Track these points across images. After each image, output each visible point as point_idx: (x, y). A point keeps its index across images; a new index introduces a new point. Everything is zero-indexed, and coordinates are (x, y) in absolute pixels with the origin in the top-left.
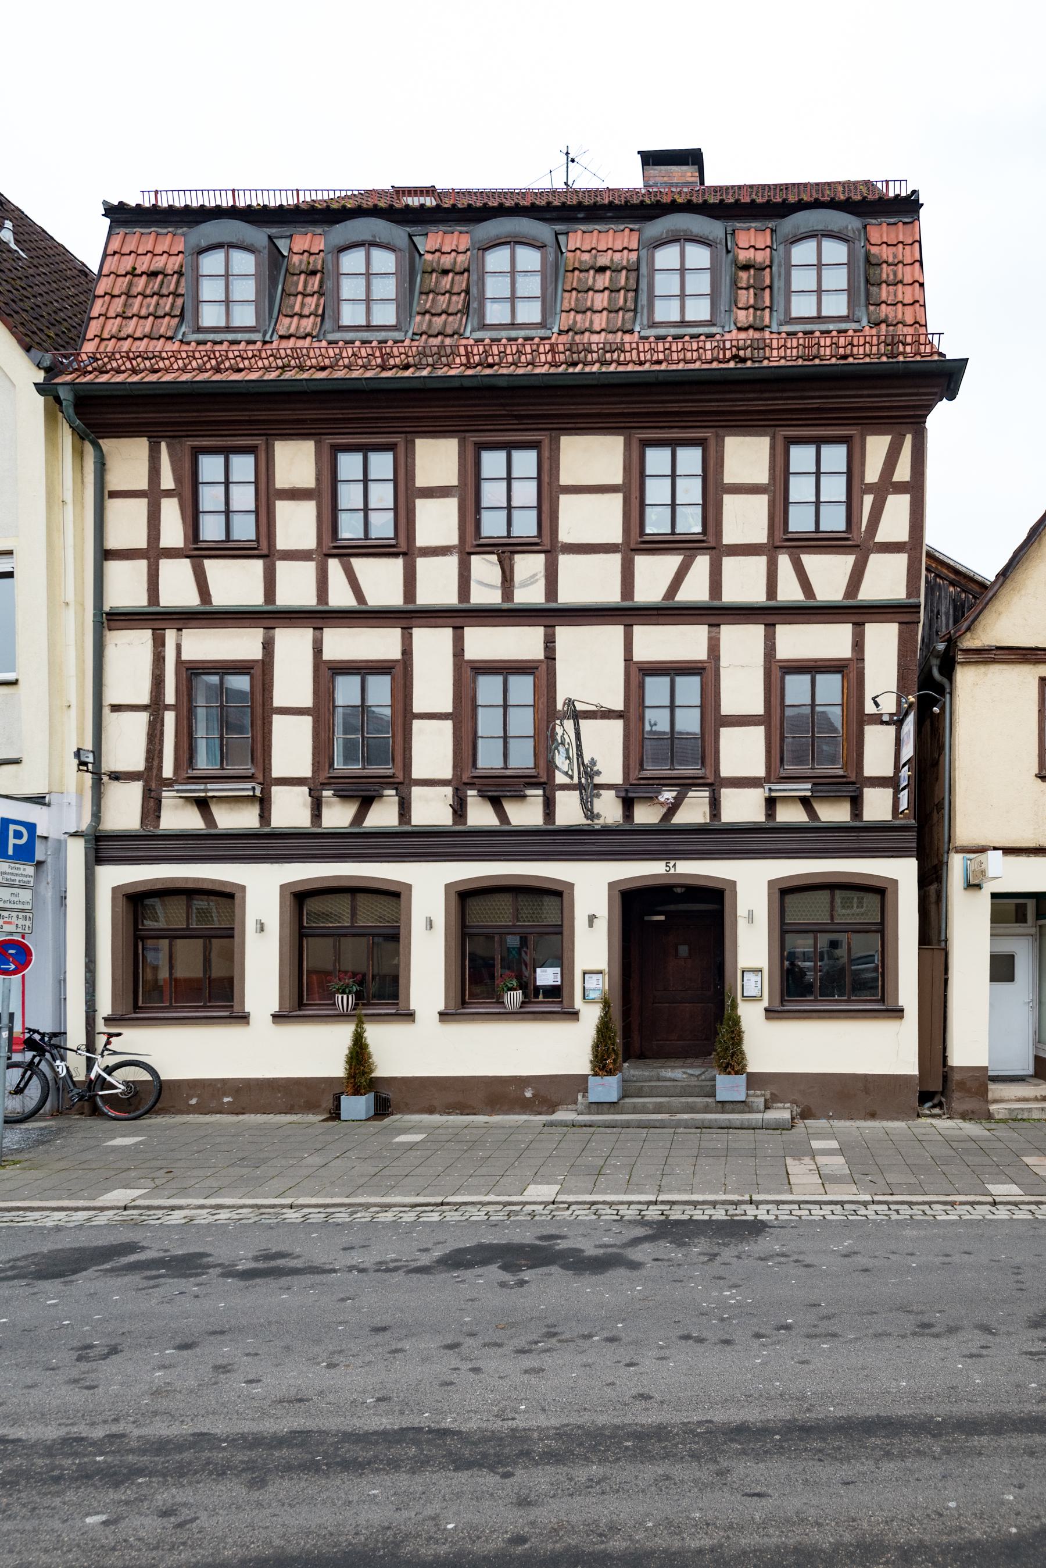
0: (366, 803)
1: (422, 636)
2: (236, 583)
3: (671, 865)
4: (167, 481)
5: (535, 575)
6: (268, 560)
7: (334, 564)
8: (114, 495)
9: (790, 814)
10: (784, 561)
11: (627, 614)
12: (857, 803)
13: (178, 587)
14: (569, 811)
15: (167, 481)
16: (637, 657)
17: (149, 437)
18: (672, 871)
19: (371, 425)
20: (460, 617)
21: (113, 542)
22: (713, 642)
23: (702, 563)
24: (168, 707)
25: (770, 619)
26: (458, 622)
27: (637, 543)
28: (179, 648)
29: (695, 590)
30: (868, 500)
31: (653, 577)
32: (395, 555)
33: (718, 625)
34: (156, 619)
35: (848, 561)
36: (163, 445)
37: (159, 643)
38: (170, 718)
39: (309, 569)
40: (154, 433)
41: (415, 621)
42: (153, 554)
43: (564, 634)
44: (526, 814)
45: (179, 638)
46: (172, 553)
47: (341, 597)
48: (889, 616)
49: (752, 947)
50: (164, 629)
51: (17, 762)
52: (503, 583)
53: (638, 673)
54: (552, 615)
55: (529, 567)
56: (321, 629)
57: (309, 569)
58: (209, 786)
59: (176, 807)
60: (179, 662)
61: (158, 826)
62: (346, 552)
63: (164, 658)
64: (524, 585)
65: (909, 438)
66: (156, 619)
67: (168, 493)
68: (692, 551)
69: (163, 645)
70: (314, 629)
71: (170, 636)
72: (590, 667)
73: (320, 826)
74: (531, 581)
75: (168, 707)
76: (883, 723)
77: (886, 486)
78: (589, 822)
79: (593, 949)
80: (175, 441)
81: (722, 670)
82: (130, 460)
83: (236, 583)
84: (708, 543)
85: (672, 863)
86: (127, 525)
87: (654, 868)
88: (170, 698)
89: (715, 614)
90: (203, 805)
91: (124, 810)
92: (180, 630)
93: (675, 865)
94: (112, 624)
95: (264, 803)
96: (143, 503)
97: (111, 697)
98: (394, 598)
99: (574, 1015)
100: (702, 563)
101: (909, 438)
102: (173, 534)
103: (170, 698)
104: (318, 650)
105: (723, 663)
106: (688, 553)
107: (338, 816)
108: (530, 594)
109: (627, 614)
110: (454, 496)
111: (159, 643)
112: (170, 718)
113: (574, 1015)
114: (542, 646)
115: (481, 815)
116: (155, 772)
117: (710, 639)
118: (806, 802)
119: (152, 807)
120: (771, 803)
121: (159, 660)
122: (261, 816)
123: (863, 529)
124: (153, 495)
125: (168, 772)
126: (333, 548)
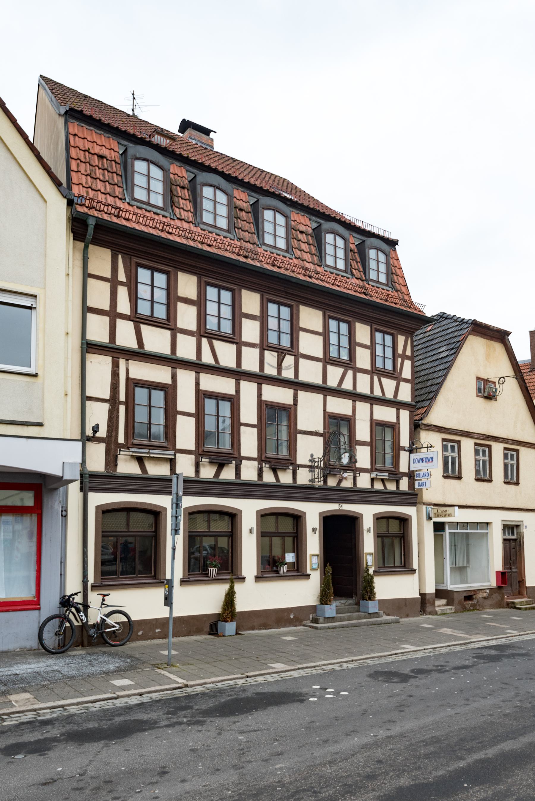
0: (221, 467)
2: (156, 340)
4: (122, 277)
5: (290, 365)
6: (173, 331)
7: (204, 341)
9: (378, 486)
11: (323, 390)
13: (126, 336)
14: (304, 477)
16: (328, 410)
17: (112, 250)
21: (90, 303)
24: (121, 403)
25: (372, 402)
26: (260, 381)
29: (347, 385)
31: (334, 374)
32: (233, 343)
33: (355, 401)
34: (113, 351)
36: (120, 257)
38: (122, 409)
39: (193, 340)
43: (302, 395)
45: (127, 364)
46: (123, 317)
47: (207, 358)
49: (369, 544)
50: (119, 358)
52: (278, 366)
55: (289, 360)
56: (199, 373)
59: (126, 460)
60: (128, 379)
61: (116, 470)
62: (212, 336)
63: (118, 375)
64: (286, 369)
66: (113, 351)
67: (122, 284)
69: (118, 366)
70: (196, 372)
71: (122, 363)
73: (199, 477)
74: (288, 368)
76: (405, 450)
78: (311, 483)
79: (313, 544)
80: (125, 256)
81: (357, 421)
83: (156, 340)
88: (122, 398)
90: (140, 460)
94: (90, 350)
95: (172, 462)
99: (308, 576)
100: (350, 373)
101: (410, 339)
102: (124, 306)
103: (122, 398)
104: (197, 384)
105: (357, 417)
106: (345, 368)
107: (208, 472)
108: (288, 374)
110: (257, 320)
111: (115, 366)
114: (292, 398)
116: (113, 439)
118: (383, 480)
119: (111, 460)
120: (372, 480)
121: (115, 375)
122: (171, 470)
124: (114, 282)
125: (121, 439)
126: (202, 333)
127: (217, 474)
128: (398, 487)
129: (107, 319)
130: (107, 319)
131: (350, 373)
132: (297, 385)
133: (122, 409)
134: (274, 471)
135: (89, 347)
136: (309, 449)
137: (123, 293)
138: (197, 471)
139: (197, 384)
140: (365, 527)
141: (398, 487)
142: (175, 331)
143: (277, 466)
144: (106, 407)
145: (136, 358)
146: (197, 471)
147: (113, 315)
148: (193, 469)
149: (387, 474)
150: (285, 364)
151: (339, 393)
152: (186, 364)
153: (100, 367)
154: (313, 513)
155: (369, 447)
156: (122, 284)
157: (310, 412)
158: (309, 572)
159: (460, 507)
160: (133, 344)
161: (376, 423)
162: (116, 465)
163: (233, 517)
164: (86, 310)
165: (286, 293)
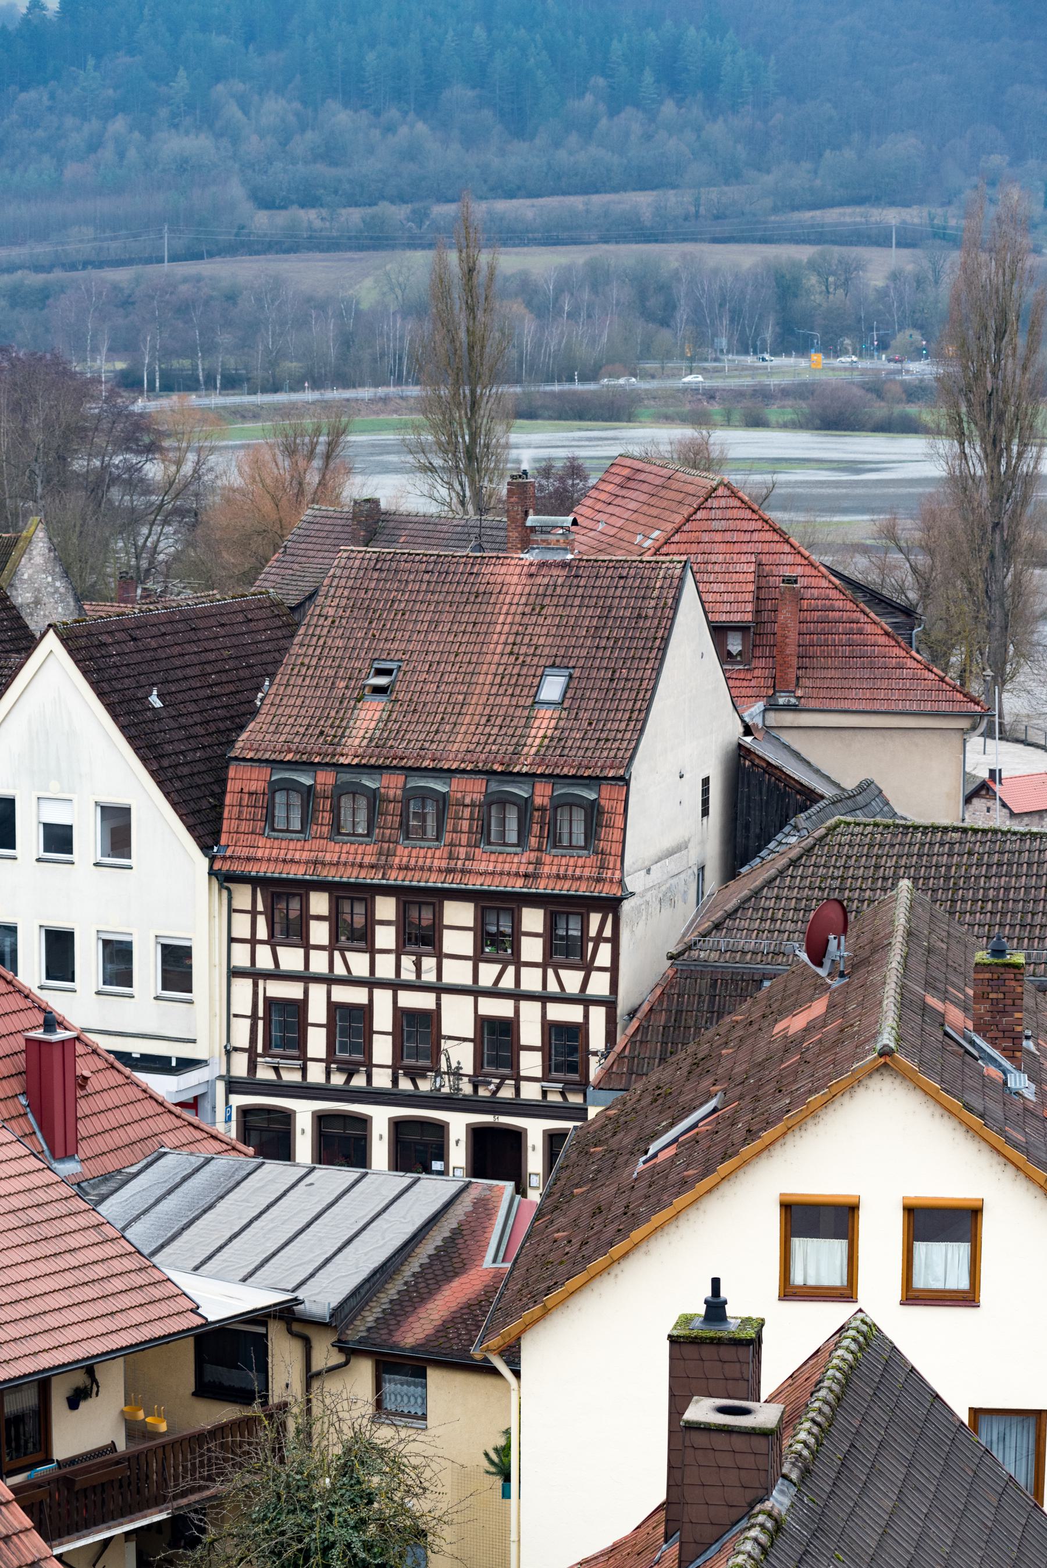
1: (378, 993)
4: (260, 907)
9: (554, 1098)
10: (550, 972)
11: (475, 992)
15: (260, 907)
20: (396, 986)
21: (234, 935)
29: (508, 982)
34: (255, 975)
38: (261, 1023)
39: (325, 955)
42: (253, 942)
43: (445, 998)
47: (340, 970)
57: (325, 955)
60: (265, 998)
65: (610, 917)
66: (255, 975)
67: (261, 913)
71: (261, 983)
74: (429, 970)
86: (242, 926)
88: (261, 1014)
89: (517, 996)
90: (276, 1069)
91: (240, 1067)
95: (304, 1070)
96: (248, 917)
98: (365, 973)
100: (511, 970)
101: (610, 917)
103: (261, 1014)
105: (521, 1019)
107: (338, 1079)
108: (429, 977)
111: (255, 985)
119: (252, 1067)
124: (254, 913)
125: (260, 1050)
127: (348, 1081)
129: (248, 946)
130: (248, 946)
131: (511, 970)
132: (439, 989)
133: (261, 1023)
135: (234, 973)
137: (261, 921)
140: (530, 1144)
142: (307, 947)
143: (414, 1075)
144: (248, 1022)
147: (253, 942)
150: (424, 967)
152: (318, 979)
153: (243, 988)
156: (261, 913)
157: (458, 1018)
160: (271, 966)
163: (364, 1122)
164: (231, 940)
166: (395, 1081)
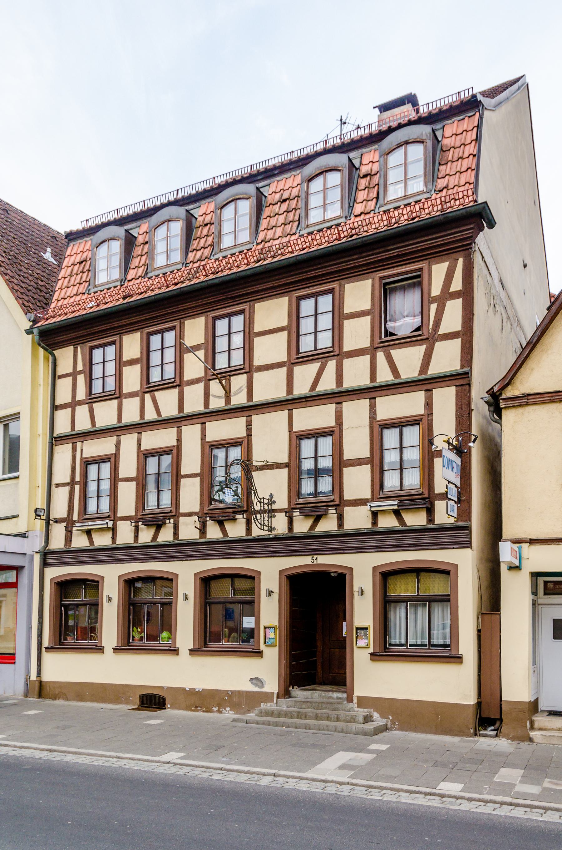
2: (106, 414)
3: (314, 558)
5: (241, 387)
8: (60, 377)
9: (388, 522)
10: (380, 356)
11: (290, 403)
12: (430, 511)
16: (295, 429)
18: (315, 562)
19: (163, 318)
21: (58, 402)
22: (339, 414)
23: (332, 365)
25: (372, 395)
27: (297, 358)
28: (82, 450)
29: (328, 383)
30: (434, 307)
33: (341, 403)
35: (421, 349)
37: (74, 449)
38: (77, 488)
39: (136, 401)
40: (74, 342)
41: (184, 423)
43: (257, 420)
44: (236, 530)
45: (82, 446)
48: (448, 383)
49: (362, 611)
51: (17, 516)
52: (225, 395)
53: (297, 438)
54: (250, 409)
55: (238, 382)
56: (141, 433)
58: (90, 523)
59: (78, 535)
64: (236, 394)
68: (325, 359)
71: (79, 445)
72: (270, 438)
74: (239, 391)
75: (76, 483)
77: (447, 295)
79: (270, 612)
80: (83, 345)
81: (344, 432)
82: (66, 357)
84: (336, 353)
85: (315, 557)
87: (306, 560)
88: (77, 479)
90: (88, 533)
92: (82, 442)
93: (316, 559)
97: (55, 481)
104: (139, 445)
106: (324, 360)
109: (290, 403)
112: (77, 488)
113: (259, 654)
115: (214, 532)
117: (336, 412)
120: (375, 515)
123: (431, 327)
125: (75, 518)
127: (155, 538)
128: (431, 520)
134: (221, 523)
136: (272, 486)
138: (136, 537)
139: (139, 445)
141: (431, 520)
145: (89, 437)
146: (136, 537)
148: (132, 535)
149: (396, 502)
151: (313, 399)
154: (270, 572)
155: (369, 466)
158: (262, 647)
159: (532, 542)
161: (380, 425)
162: (71, 541)
165: (232, 298)
166: (203, 531)
